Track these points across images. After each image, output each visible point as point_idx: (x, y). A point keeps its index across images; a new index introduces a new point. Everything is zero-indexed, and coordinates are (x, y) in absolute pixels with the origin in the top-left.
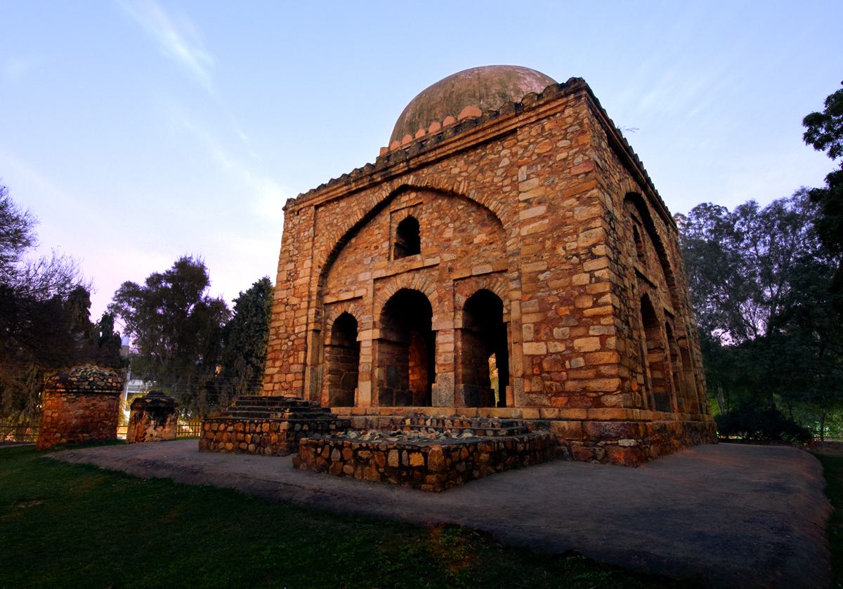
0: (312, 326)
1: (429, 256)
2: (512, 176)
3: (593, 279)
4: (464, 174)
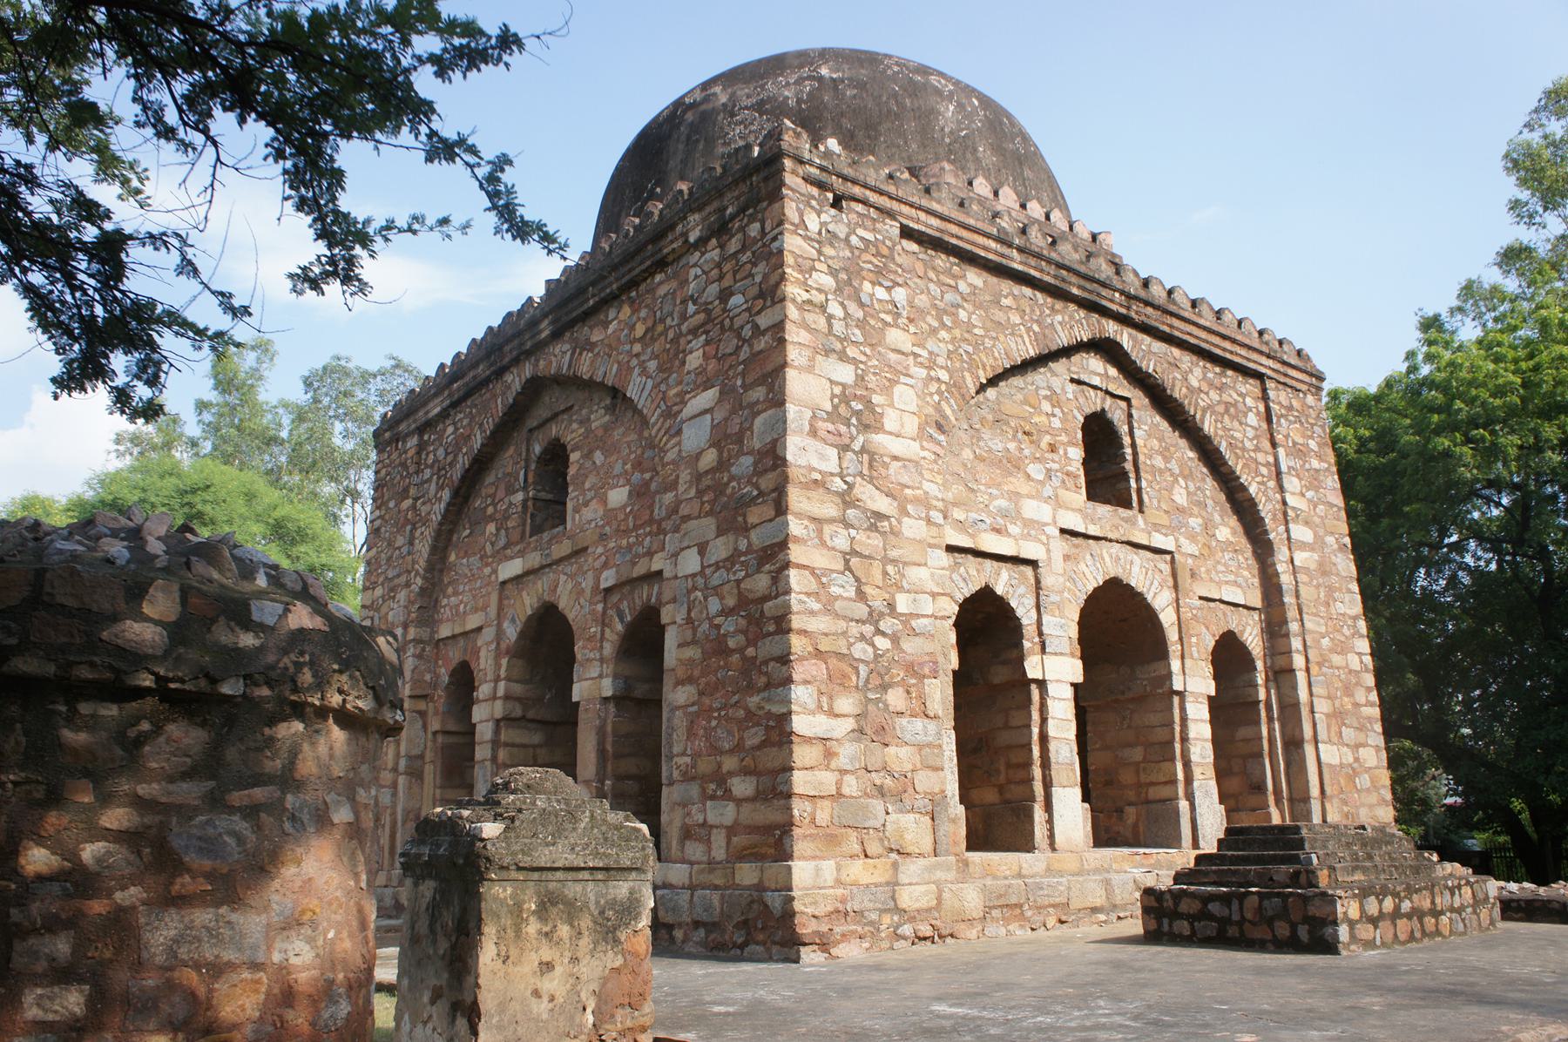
1: (1157, 527)
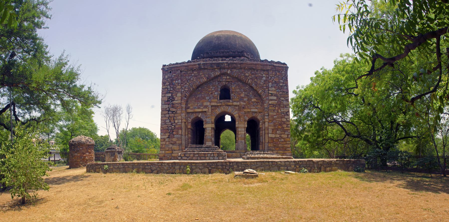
0: (184, 120)
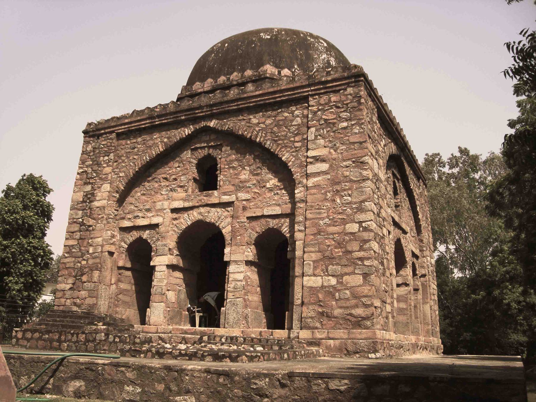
1: (225, 194)
2: (303, 134)
3: (361, 229)
4: (262, 125)
